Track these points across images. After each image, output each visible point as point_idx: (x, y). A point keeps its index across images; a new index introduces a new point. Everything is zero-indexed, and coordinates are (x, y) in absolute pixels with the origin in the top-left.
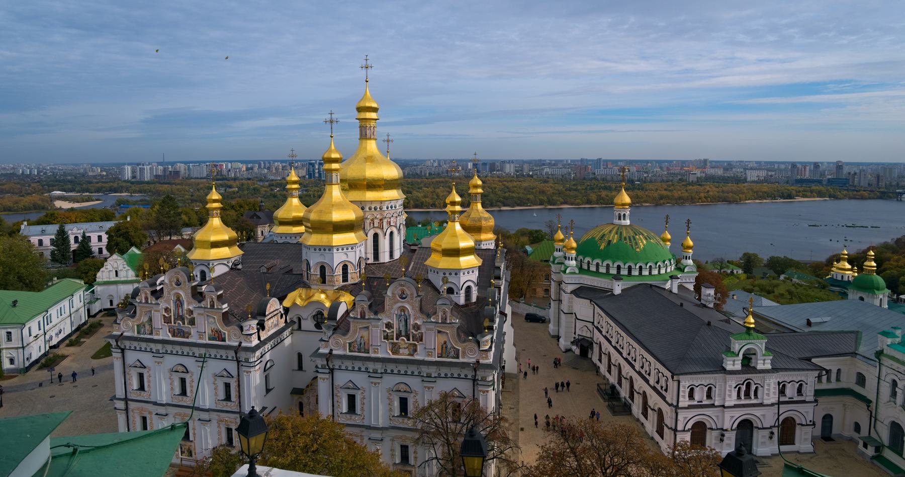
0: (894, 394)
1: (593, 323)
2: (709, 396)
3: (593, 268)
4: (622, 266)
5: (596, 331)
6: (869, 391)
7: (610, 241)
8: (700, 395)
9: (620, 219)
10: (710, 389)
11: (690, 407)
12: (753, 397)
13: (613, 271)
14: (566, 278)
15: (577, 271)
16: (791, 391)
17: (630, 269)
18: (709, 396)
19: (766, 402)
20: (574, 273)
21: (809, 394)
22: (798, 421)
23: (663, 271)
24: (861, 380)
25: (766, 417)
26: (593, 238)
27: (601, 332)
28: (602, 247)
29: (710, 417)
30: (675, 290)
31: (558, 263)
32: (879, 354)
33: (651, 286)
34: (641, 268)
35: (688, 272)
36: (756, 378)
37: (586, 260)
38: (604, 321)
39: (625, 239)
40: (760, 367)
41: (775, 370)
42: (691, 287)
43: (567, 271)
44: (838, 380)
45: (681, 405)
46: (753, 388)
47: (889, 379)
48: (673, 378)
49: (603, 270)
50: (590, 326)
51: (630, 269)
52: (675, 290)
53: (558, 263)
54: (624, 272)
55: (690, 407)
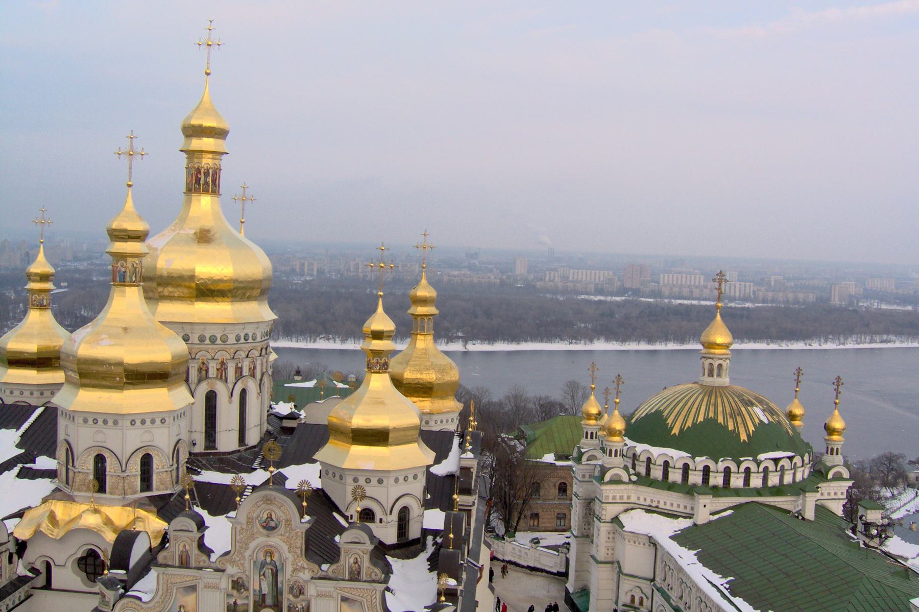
1: (653, 580)
5: (658, 597)
26: (658, 413)
27: (667, 598)
30: (810, 514)
34: (748, 470)
42: (837, 508)
50: (647, 587)
52: (810, 514)
54: (717, 480)
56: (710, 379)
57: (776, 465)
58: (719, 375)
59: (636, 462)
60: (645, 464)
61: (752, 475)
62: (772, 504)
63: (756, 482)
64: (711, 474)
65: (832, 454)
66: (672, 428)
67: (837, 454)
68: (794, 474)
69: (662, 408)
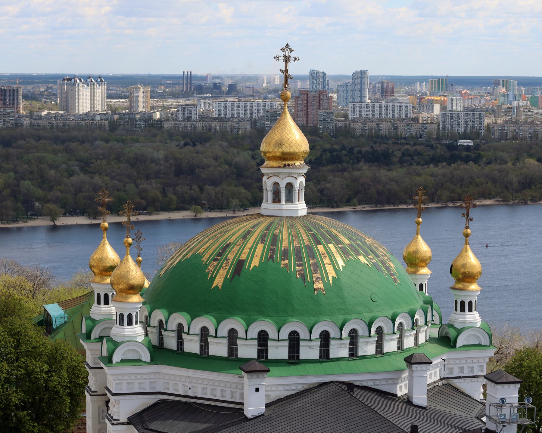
3: (192, 346)
4: (272, 334)
7: (240, 264)
9: (277, 199)
13: (248, 350)
14: (115, 378)
15: (146, 356)
17: (294, 340)
23: (390, 346)
28: (219, 281)
33: (351, 386)
39: (285, 254)
43: (116, 358)
49: (217, 348)
51: (294, 340)
52: (420, 398)
54: (279, 351)
56: (276, 206)
57: (370, 326)
58: (290, 200)
59: (163, 333)
60: (174, 335)
61: (332, 342)
62: (365, 384)
63: (339, 350)
64: (270, 343)
65: (462, 310)
66: (213, 279)
67: (470, 310)
69: (201, 250)
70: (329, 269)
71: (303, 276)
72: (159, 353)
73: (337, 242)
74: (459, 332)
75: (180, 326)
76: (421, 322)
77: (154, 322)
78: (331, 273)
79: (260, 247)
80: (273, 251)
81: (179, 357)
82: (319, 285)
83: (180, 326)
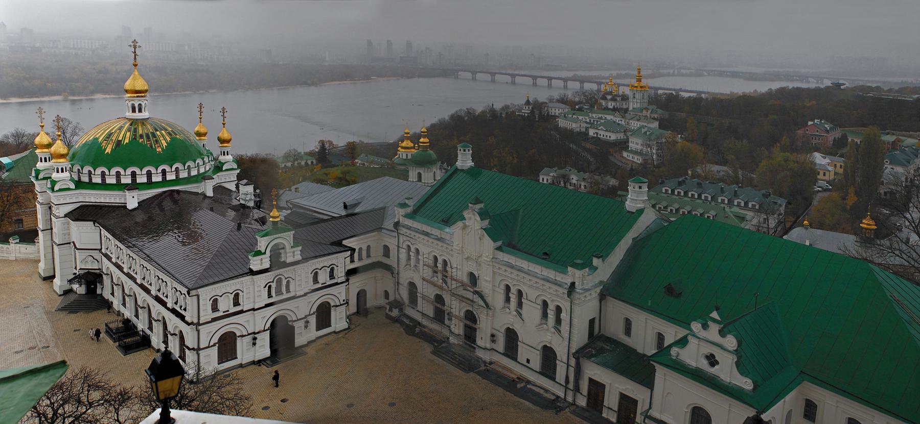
0: (409, 258)
2: (236, 303)
3: (97, 180)
6: (392, 261)
7: (119, 142)
8: (226, 305)
9: (134, 111)
10: (237, 296)
11: (214, 320)
12: (284, 292)
15: (72, 186)
16: (323, 278)
17: (149, 174)
18: (236, 303)
19: (298, 294)
20: (69, 189)
21: (340, 275)
22: (332, 304)
24: (386, 251)
25: (301, 310)
26: (96, 139)
28: (108, 150)
29: (242, 325)
30: (210, 193)
31: (45, 178)
32: (397, 224)
35: (227, 170)
36: (285, 272)
37: (86, 170)
38: (112, 244)
39: (141, 136)
40: (289, 260)
41: (305, 260)
43: (56, 188)
44: (368, 256)
45: (202, 320)
46: (284, 282)
47: (405, 246)
48: (189, 293)
49: (111, 180)
52: (210, 193)
53: (45, 178)
55: (214, 320)
63: (171, 177)
68: (198, 171)
70: (163, 142)
71: (151, 146)
72: (79, 184)
73: (166, 130)
74: (224, 164)
75: (90, 171)
76: (207, 161)
77: (75, 169)
78: (165, 144)
79: (128, 134)
80: (135, 135)
81: (91, 185)
82: (159, 150)
83: (90, 171)
